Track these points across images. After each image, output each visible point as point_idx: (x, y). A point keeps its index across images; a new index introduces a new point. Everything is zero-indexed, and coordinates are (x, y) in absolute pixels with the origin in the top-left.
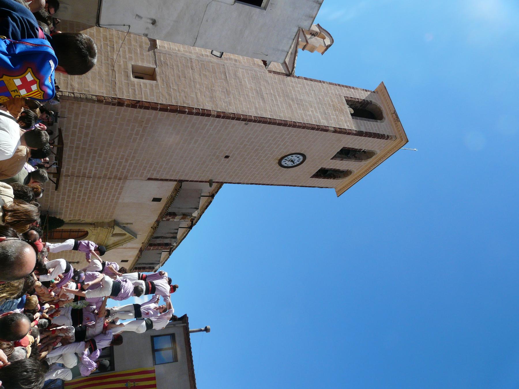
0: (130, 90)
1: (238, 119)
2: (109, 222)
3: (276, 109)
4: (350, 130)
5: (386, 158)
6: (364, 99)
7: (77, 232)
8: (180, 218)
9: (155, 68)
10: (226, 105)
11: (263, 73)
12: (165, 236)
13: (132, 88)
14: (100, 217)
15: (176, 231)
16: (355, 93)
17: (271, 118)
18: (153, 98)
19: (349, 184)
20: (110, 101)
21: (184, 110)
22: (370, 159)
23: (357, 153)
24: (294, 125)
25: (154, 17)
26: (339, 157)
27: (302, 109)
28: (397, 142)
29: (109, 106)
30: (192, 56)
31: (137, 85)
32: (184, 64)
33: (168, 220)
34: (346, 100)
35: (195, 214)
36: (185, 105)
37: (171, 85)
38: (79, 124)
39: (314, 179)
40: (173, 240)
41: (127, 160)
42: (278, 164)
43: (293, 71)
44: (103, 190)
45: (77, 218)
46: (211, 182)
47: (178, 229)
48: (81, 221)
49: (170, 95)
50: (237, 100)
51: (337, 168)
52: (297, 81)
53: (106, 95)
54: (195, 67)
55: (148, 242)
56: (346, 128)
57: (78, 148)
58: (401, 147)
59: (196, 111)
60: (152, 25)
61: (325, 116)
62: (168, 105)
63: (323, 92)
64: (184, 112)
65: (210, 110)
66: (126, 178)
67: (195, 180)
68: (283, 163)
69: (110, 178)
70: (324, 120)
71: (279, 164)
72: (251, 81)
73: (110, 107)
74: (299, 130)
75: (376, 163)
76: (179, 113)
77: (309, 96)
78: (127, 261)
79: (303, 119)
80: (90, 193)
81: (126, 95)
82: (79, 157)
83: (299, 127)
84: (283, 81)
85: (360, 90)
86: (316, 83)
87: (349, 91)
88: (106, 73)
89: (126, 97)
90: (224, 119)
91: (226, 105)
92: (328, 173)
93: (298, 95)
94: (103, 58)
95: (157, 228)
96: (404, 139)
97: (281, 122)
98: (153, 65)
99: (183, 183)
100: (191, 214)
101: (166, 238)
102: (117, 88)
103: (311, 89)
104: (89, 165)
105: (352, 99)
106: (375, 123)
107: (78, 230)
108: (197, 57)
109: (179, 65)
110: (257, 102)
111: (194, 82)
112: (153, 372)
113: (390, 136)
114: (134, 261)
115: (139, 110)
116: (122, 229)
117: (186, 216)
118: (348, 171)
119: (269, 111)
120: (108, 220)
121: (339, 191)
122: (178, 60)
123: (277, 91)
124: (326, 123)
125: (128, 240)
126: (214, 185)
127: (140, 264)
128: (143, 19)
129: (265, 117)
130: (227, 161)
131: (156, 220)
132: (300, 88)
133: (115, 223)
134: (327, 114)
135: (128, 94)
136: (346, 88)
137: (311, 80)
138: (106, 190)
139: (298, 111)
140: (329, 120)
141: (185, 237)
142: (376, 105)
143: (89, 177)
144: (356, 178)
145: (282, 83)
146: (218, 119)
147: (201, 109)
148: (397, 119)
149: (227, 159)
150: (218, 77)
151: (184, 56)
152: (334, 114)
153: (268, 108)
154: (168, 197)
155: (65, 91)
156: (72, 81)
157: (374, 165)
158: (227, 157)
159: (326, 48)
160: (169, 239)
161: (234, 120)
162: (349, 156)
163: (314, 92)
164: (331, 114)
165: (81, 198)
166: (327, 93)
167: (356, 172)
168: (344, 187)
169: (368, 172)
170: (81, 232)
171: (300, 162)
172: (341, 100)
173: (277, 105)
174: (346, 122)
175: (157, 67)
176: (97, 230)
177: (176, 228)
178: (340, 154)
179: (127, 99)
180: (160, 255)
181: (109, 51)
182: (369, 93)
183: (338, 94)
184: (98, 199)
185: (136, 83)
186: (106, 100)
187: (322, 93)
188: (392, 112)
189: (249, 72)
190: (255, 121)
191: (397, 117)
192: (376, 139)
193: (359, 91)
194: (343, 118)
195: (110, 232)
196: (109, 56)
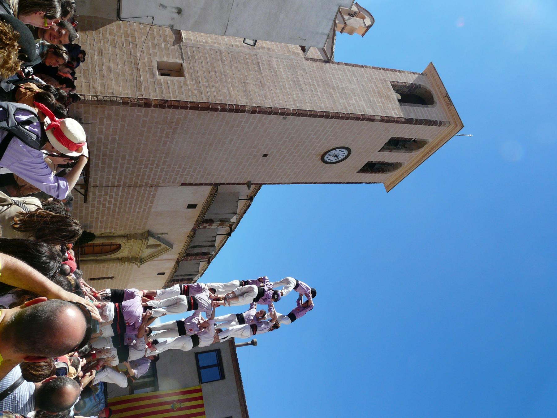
0: (157, 89)
1: (276, 113)
2: (142, 233)
3: (317, 100)
4: (399, 118)
5: (439, 147)
6: (411, 82)
7: (109, 245)
8: (217, 225)
9: (182, 64)
10: (261, 98)
11: (299, 61)
12: (202, 244)
13: (159, 86)
14: (132, 228)
15: (214, 239)
16: (402, 76)
17: (311, 111)
18: (182, 96)
19: (399, 177)
20: (136, 102)
21: (216, 107)
22: (422, 148)
23: (407, 143)
24: (337, 116)
25: (179, 6)
26: (387, 149)
27: (344, 98)
28: (451, 128)
29: (135, 107)
30: (221, 48)
31: (164, 83)
32: (213, 56)
33: (205, 227)
34: (391, 85)
35: (234, 220)
36: (217, 102)
37: (201, 81)
38: (104, 130)
39: (360, 174)
40: (212, 249)
41: (157, 166)
42: (321, 160)
43: (332, 57)
44: (134, 200)
45: (108, 231)
46: (249, 184)
47: (216, 237)
48: (113, 233)
49: (200, 92)
50: (273, 92)
51: (386, 161)
52: (337, 67)
53: (131, 96)
54: (225, 59)
55: (185, 252)
56: (394, 116)
57: (104, 155)
58: (455, 134)
59: (230, 108)
60: (177, 14)
61: (370, 105)
62: (198, 103)
63: (366, 78)
64: (216, 110)
65: (244, 105)
66: (158, 185)
67: (232, 183)
68: (326, 159)
69: (140, 186)
70: (369, 109)
71: (322, 161)
72: (287, 70)
73: (137, 109)
74: (343, 121)
75: (428, 153)
76: (210, 111)
77: (351, 83)
78: (163, 274)
79: (346, 109)
80: (121, 202)
81: (153, 95)
82: (106, 165)
83: (342, 118)
84: (322, 68)
85: (406, 73)
86: (358, 68)
87: (395, 75)
88: (130, 72)
89: (153, 97)
90: (261, 115)
91: (261, 98)
92: (374, 168)
93: (339, 83)
94: (125, 55)
95: (193, 237)
96: (458, 125)
97: (322, 114)
98: (180, 59)
99: (220, 187)
100: (230, 219)
101: (204, 247)
102: (143, 88)
103: (353, 76)
104: (118, 173)
105: (398, 84)
106: (426, 108)
107: (110, 244)
108: (226, 48)
109: (208, 58)
110: (294, 93)
111: (225, 75)
112: (200, 390)
113: (443, 121)
114: (171, 273)
115: (168, 110)
116: (156, 239)
117: (224, 223)
118: (398, 163)
119: (308, 102)
120: (140, 231)
121: (388, 186)
122: (206, 53)
123: (316, 80)
124: (372, 113)
125: (163, 252)
126: (253, 187)
127: (177, 276)
128: (167, 8)
129: (305, 109)
130: (265, 160)
131: (192, 229)
132: (341, 75)
133: (149, 234)
134: (372, 102)
135: (155, 94)
136: (391, 72)
137: (352, 65)
138: (137, 199)
139: (340, 100)
140: (375, 108)
141: (224, 244)
142: (424, 88)
143: (118, 186)
144: (407, 171)
145: (321, 71)
146: (253, 115)
147: (235, 105)
148: (450, 102)
149: (265, 158)
150: (250, 69)
151: (212, 48)
152: (380, 102)
153: (307, 100)
154: (204, 203)
155: (87, 94)
156: (95, 84)
157: (426, 155)
158: (265, 156)
159: (366, 28)
160: (207, 248)
161: (271, 115)
162: (398, 146)
163: (356, 78)
164: (377, 102)
165: (112, 210)
166: (370, 78)
167: (406, 164)
168: (394, 182)
169: (421, 163)
170: (114, 245)
171: (344, 156)
172: (386, 85)
173: (317, 95)
174: (394, 110)
175: (183, 62)
176: (130, 242)
177: (214, 236)
178: (388, 146)
179: (154, 99)
180: (198, 265)
181: (131, 48)
182: (417, 76)
183: (382, 79)
184: (130, 208)
185: (162, 81)
186: (132, 101)
187: (366, 79)
188: (445, 95)
189: (284, 61)
190: (294, 115)
191: (450, 101)
192: (427, 127)
193: (406, 75)
194: (390, 105)
195: (144, 244)
196: (132, 53)
